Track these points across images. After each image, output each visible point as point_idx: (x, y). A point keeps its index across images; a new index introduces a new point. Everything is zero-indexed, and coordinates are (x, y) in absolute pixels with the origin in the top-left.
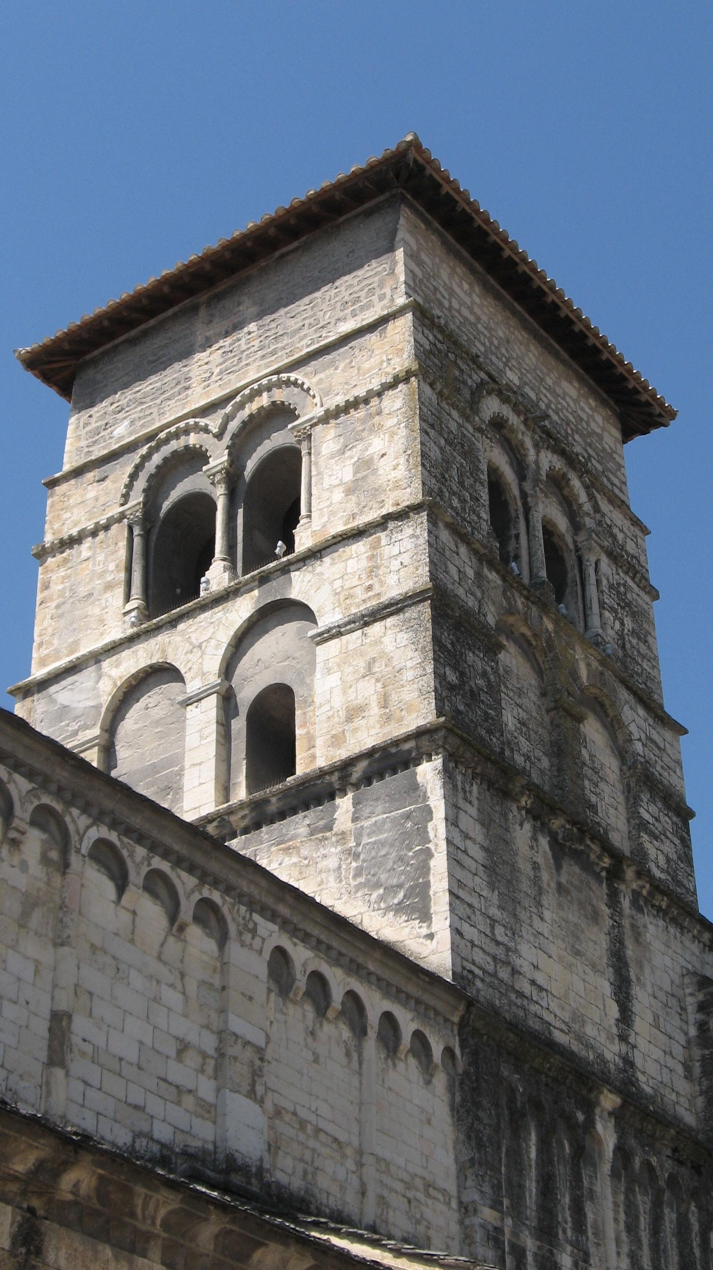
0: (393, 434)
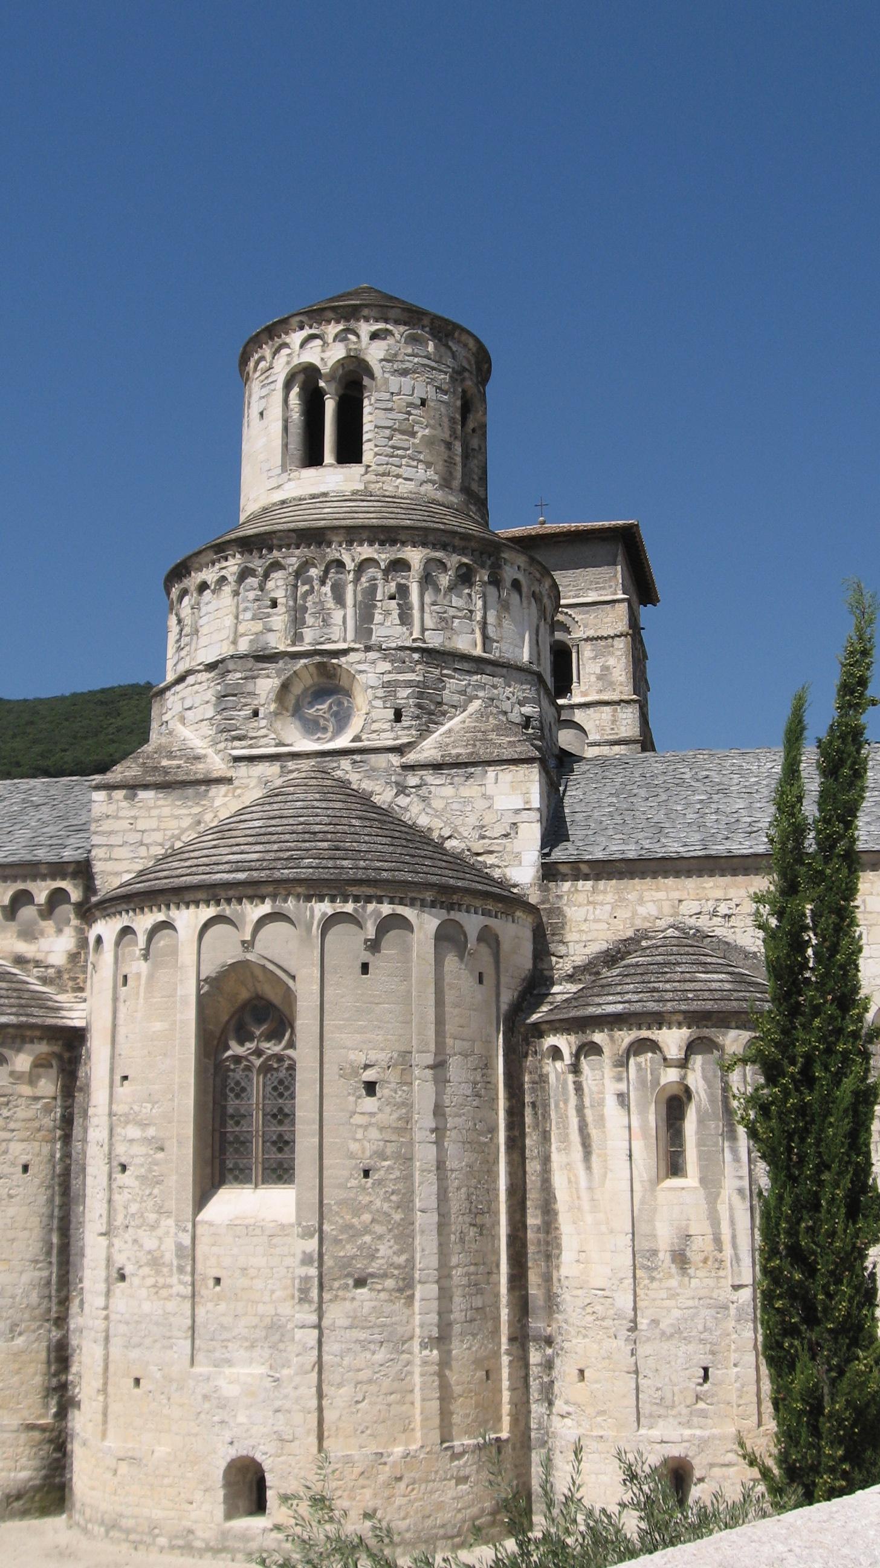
0: (619, 660)
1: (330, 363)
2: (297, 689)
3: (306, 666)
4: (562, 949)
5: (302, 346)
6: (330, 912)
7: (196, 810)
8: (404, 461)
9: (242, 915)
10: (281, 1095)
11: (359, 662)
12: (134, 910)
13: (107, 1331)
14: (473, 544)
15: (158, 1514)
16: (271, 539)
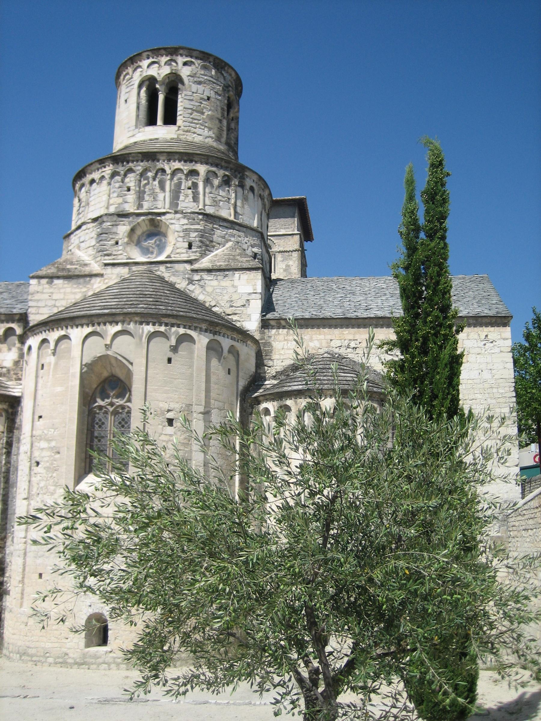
0: (294, 262)
1: (162, 76)
2: (139, 232)
3: (144, 220)
4: (270, 363)
5: (148, 67)
6: (152, 330)
7: (84, 290)
8: (198, 126)
9: (106, 331)
10: (123, 426)
11: (171, 219)
12: (49, 330)
13: (25, 549)
14: (231, 166)
15: (48, 645)
16: (129, 157)
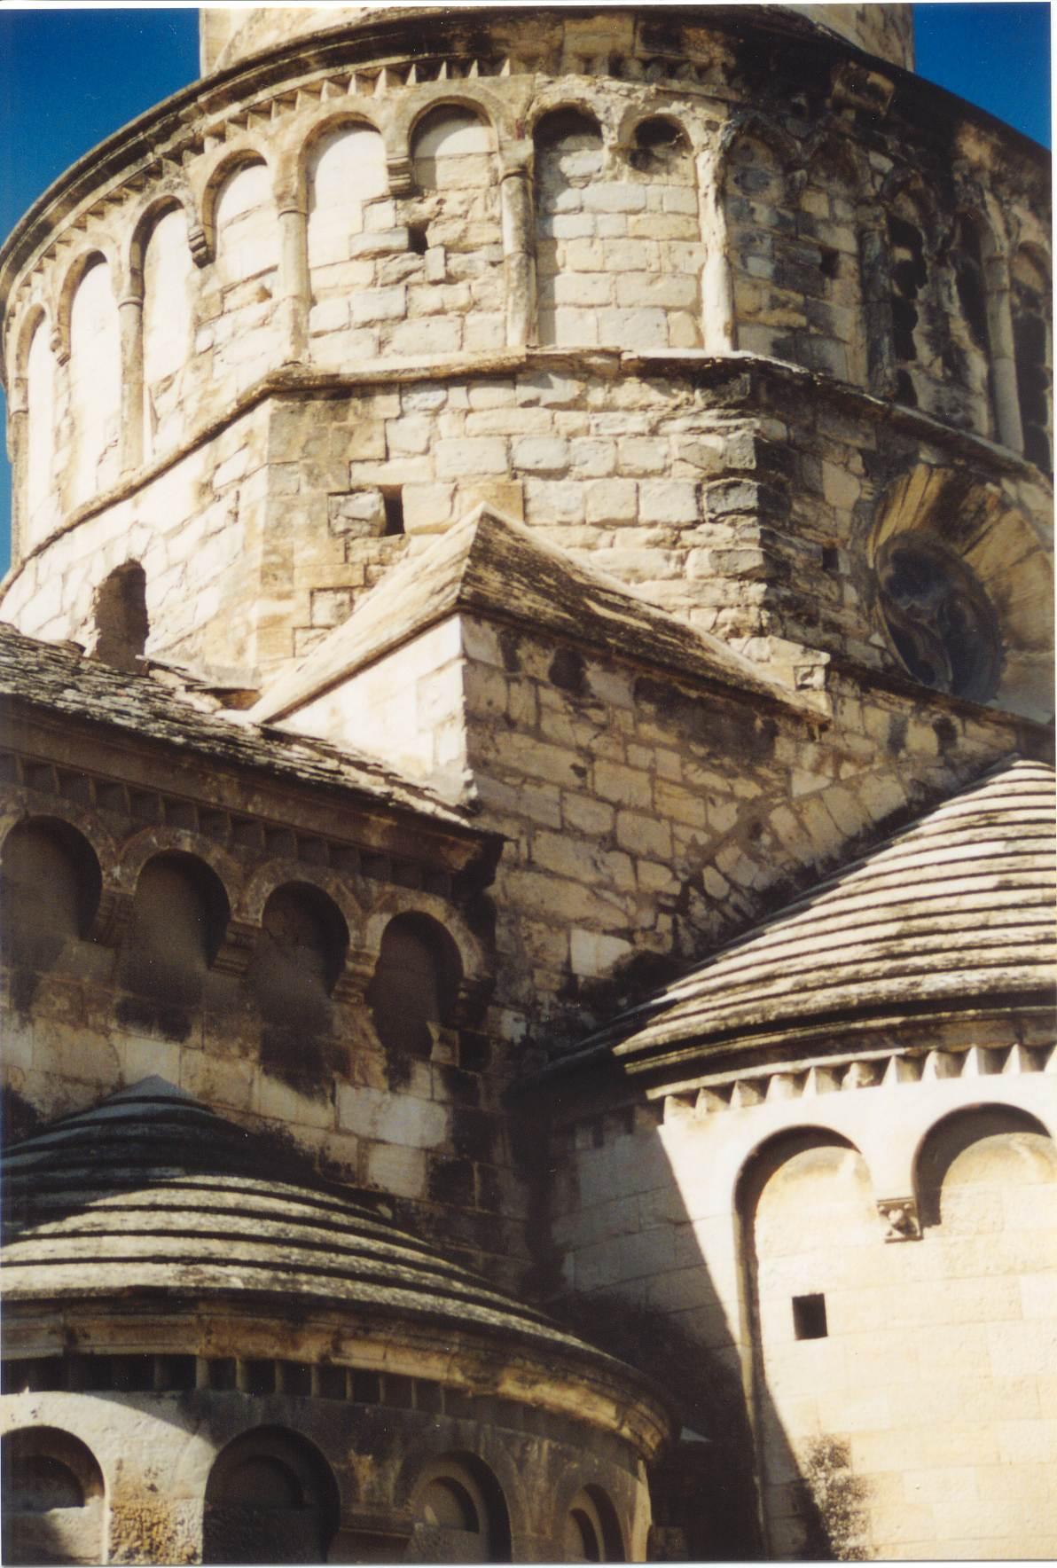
7: (747, 789)
